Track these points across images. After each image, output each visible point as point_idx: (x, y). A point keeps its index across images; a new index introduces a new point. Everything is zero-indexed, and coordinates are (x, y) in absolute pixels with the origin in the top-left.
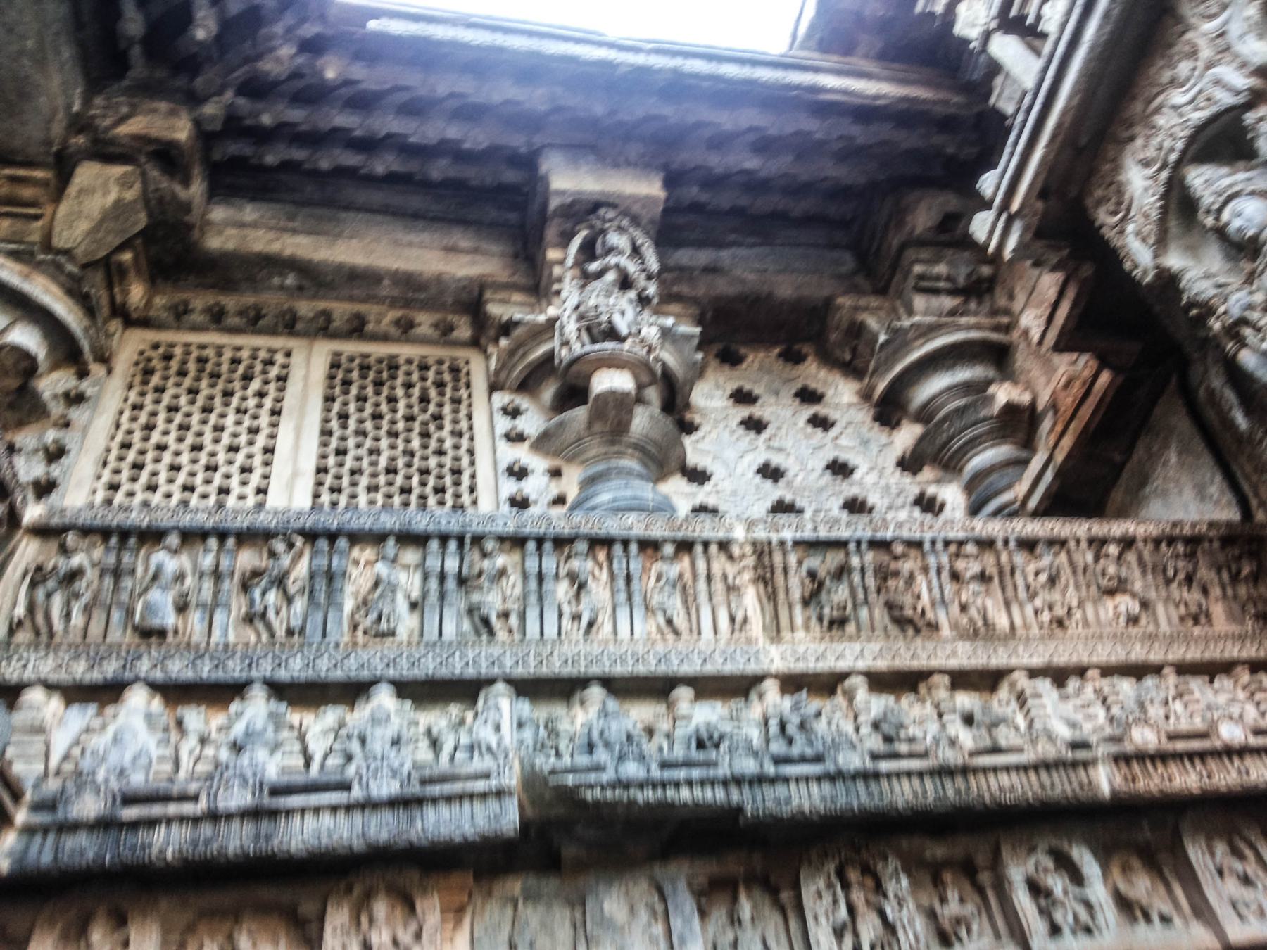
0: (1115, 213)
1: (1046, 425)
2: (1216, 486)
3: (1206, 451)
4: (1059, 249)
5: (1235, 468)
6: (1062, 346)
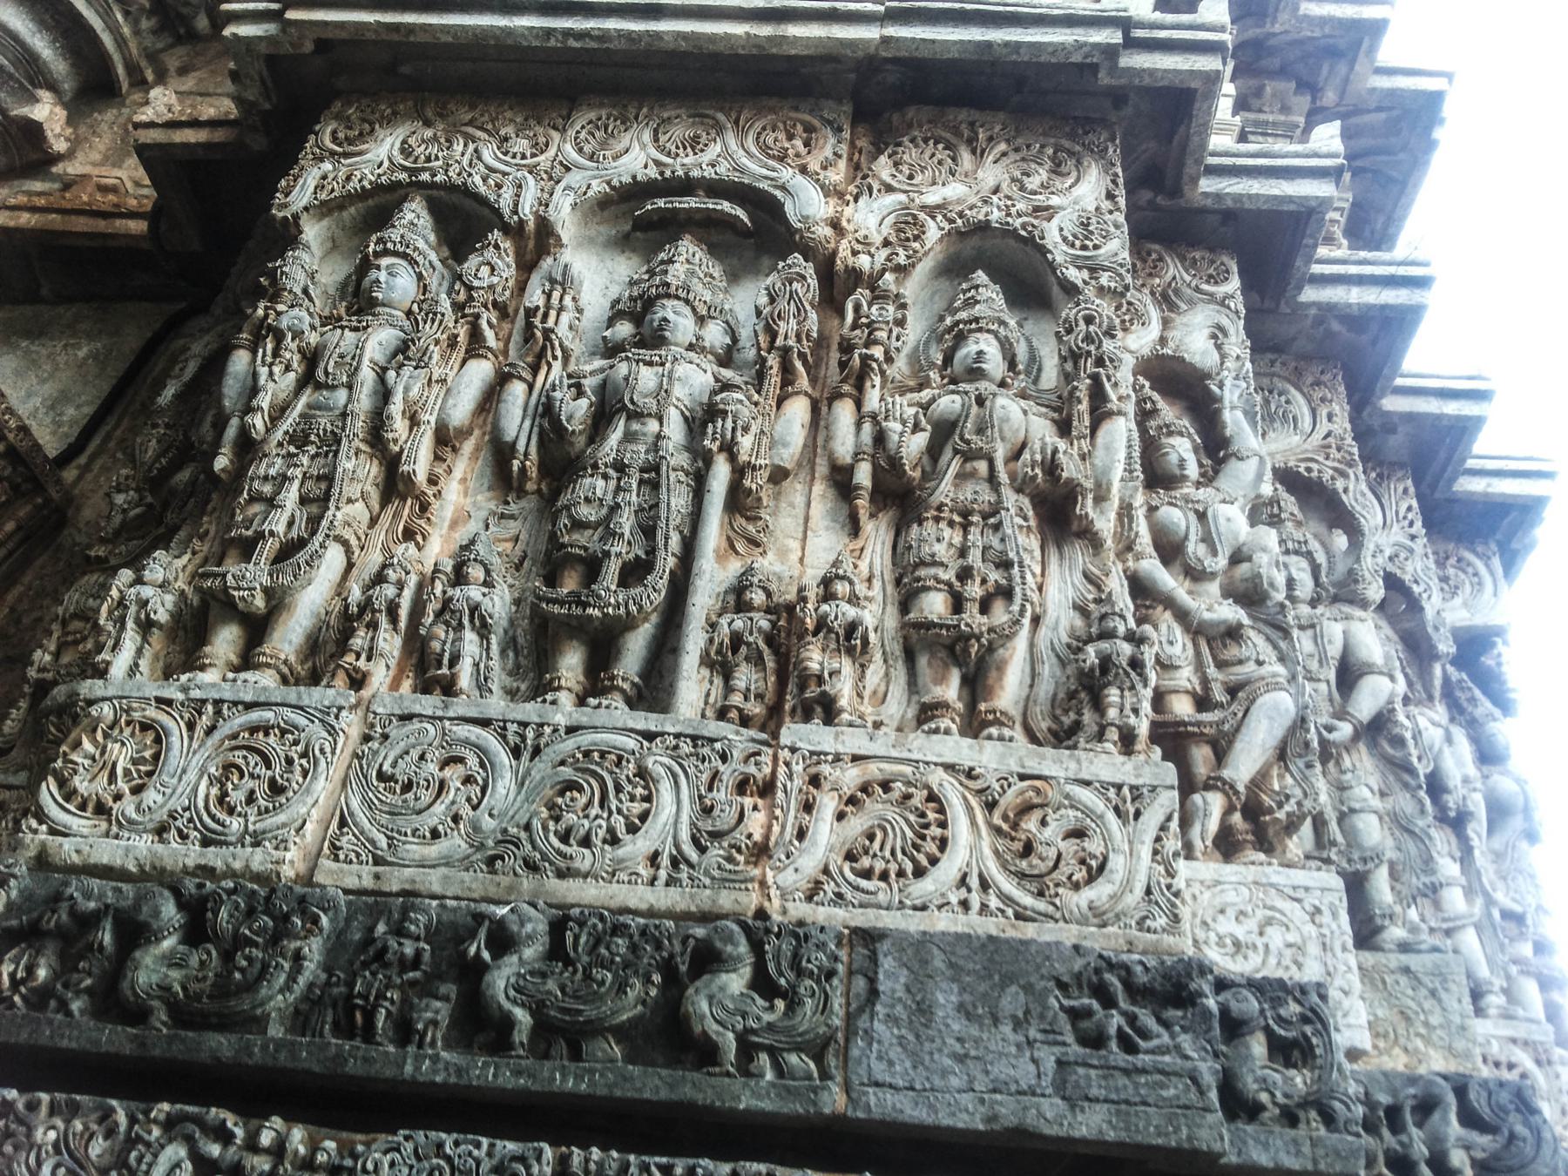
0: (335, 139)
1: (38, 186)
2: (75, 413)
3: (114, 381)
4: (268, 98)
5: (111, 421)
6: (151, 156)
